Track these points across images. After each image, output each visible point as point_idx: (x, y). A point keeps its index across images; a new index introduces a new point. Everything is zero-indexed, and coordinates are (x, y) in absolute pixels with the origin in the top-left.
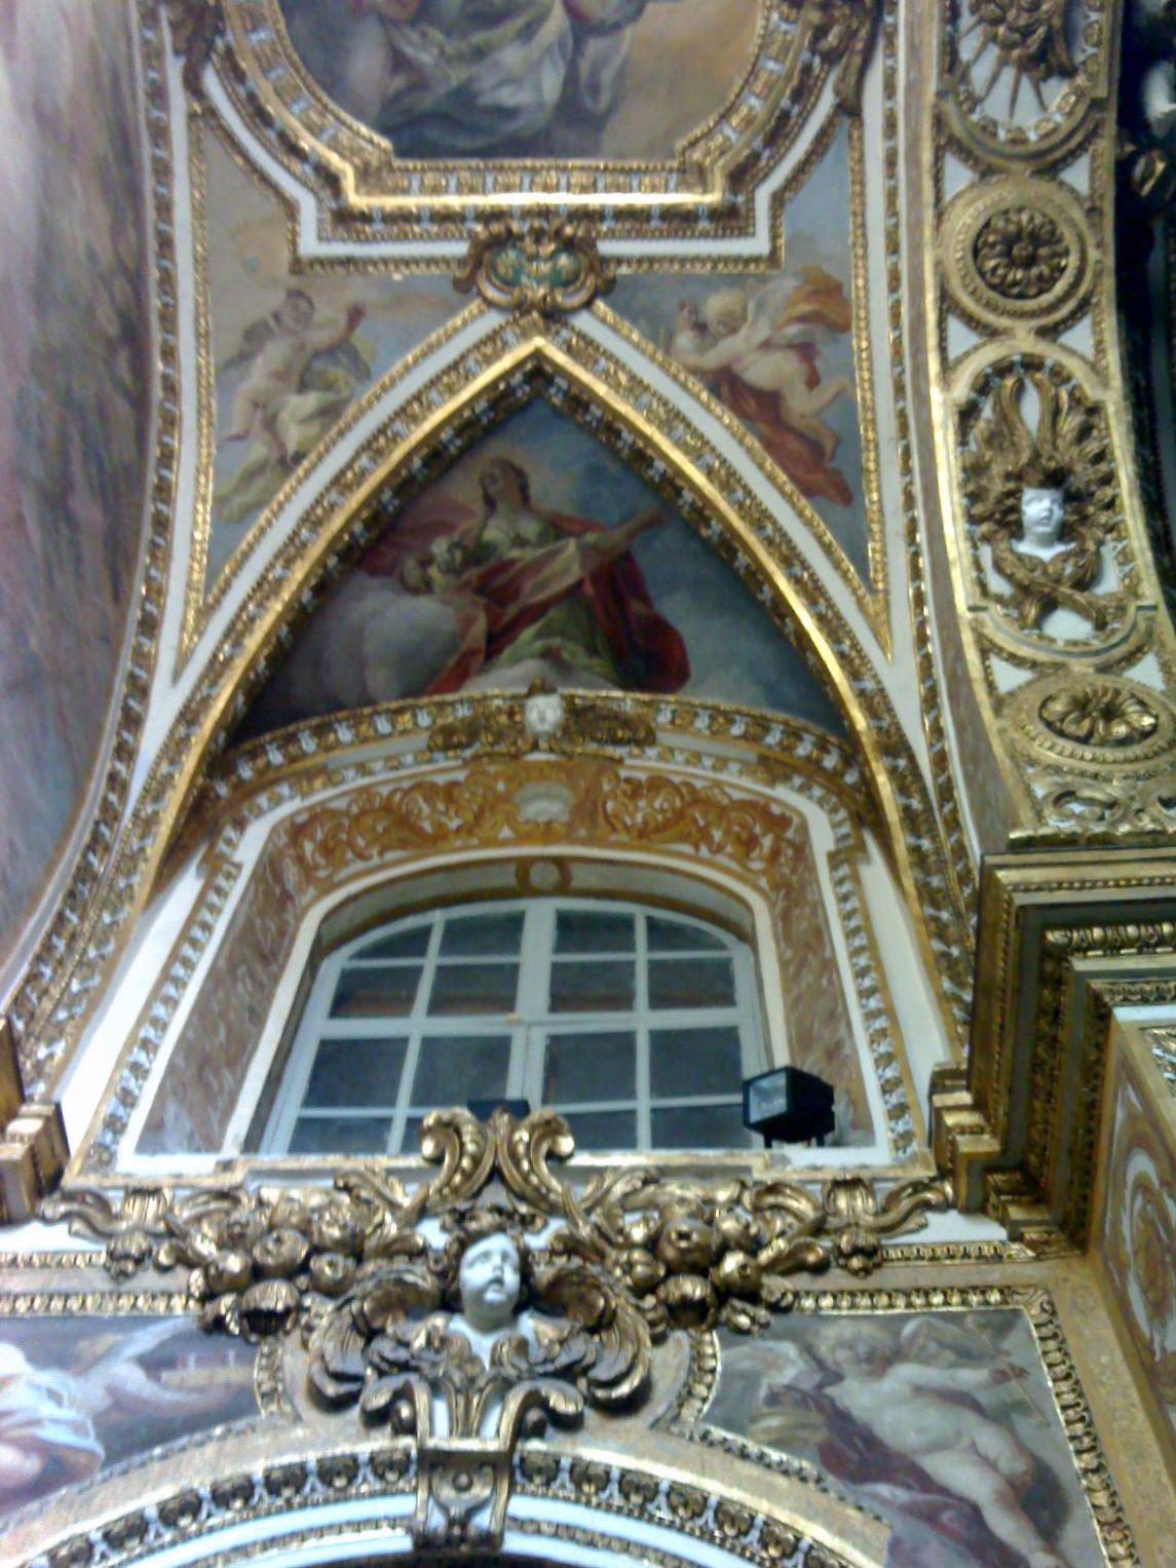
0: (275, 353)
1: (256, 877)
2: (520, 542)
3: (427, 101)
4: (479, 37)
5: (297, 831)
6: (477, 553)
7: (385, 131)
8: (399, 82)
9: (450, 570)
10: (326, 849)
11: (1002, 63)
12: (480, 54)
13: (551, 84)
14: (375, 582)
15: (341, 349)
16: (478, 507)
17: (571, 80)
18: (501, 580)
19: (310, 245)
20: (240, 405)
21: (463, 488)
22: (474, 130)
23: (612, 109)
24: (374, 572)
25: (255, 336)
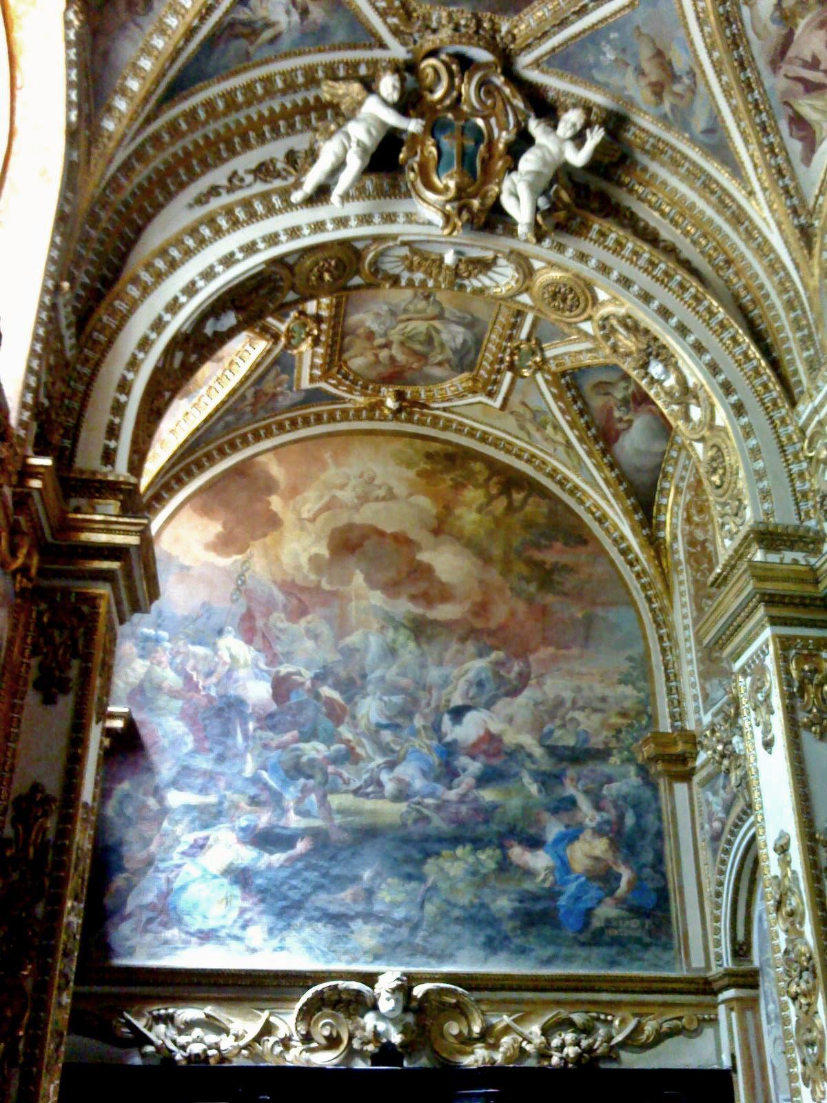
0: (531, 427)
1: (688, 562)
2: (626, 388)
3: (455, 360)
4: (436, 343)
5: (688, 520)
6: (625, 402)
7: (462, 371)
8: (447, 366)
9: (627, 413)
10: (701, 511)
11: (486, 275)
12: (442, 345)
13: (460, 329)
14: (620, 440)
15: (535, 414)
16: (606, 398)
17: (458, 323)
18: (639, 398)
19: (498, 403)
20: (545, 443)
21: (597, 402)
22: (468, 352)
23: (472, 315)
24: (616, 439)
25: (522, 428)
